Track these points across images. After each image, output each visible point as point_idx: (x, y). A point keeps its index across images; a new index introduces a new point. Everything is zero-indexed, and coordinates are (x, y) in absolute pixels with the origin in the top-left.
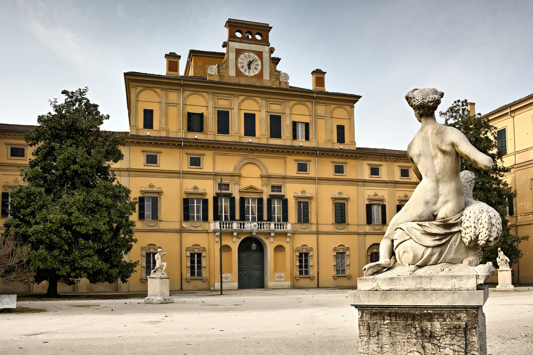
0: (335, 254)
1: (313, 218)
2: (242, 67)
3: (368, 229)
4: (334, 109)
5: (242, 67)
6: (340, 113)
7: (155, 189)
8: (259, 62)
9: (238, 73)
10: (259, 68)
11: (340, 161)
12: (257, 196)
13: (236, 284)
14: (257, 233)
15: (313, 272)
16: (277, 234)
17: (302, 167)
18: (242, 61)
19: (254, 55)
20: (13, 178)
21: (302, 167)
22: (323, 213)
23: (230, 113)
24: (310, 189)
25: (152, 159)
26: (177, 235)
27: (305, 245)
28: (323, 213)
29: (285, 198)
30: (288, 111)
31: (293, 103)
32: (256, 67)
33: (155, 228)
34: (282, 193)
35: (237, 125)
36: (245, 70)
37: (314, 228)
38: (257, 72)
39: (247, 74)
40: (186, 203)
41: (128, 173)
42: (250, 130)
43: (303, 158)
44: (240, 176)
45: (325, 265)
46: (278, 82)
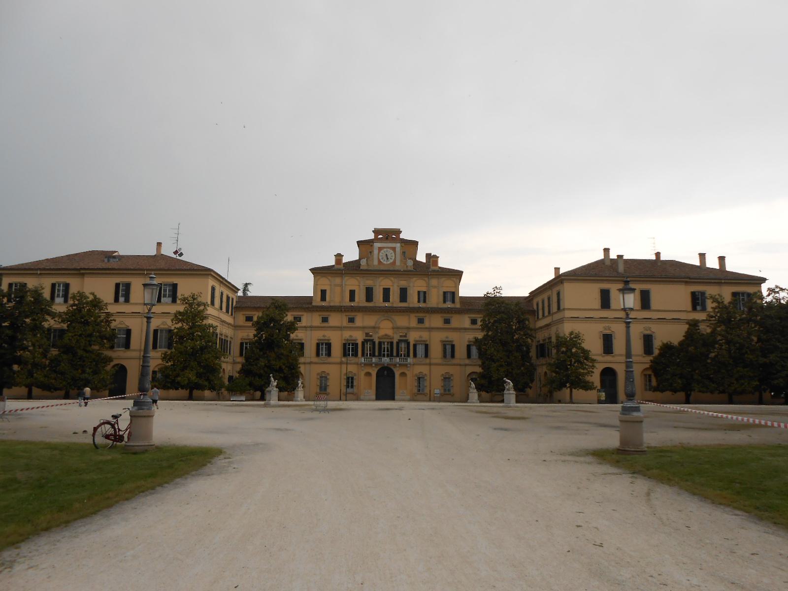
0: (442, 378)
3: (467, 361)
5: (382, 258)
6: (447, 284)
7: (326, 338)
8: (393, 254)
9: (380, 262)
10: (393, 258)
11: (447, 316)
12: (390, 340)
13: (374, 397)
14: (388, 364)
15: (427, 391)
16: (400, 365)
17: (421, 321)
20: (246, 334)
21: (421, 321)
22: (436, 351)
25: (325, 320)
26: (339, 366)
27: (421, 372)
29: (409, 341)
30: (411, 285)
31: (415, 279)
33: (326, 361)
34: (407, 338)
35: (378, 295)
38: (392, 261)
41: (310, 329)
42: (386, 298)
43: (421, 315)
44: (379, 328)
46: (406, 266)
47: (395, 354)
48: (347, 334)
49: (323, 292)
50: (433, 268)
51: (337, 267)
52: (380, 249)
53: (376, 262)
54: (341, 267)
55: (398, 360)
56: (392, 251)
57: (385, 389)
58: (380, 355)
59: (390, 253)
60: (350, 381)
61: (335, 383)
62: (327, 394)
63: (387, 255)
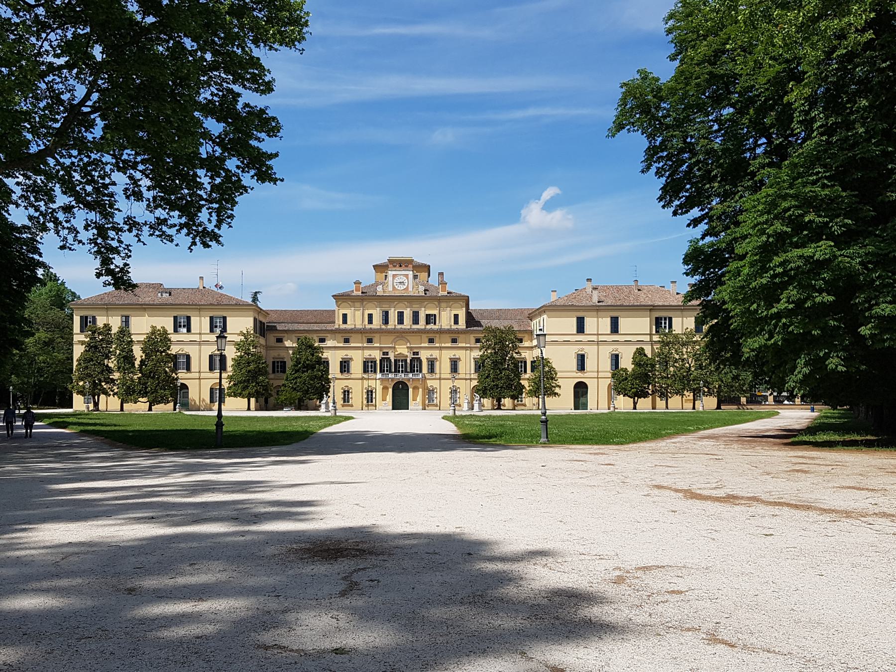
1: (437, 369)
16: (413, 380)
22: (444, 367)
24: (435, 354)
28: (444, 367)
37: (438, 376)
40: (366, 365)
42: (401, 321)
45: (444, 397)
47: (409, 370)
48: (367, 353)
49: (345, 316)
50: (441, 293)
51: (355, 293)
52: (394, 276)
53: (390, 289)
54: (360, 293)
55: (410, 375)
57: (400, 402)
58: (397, 371)
59: (404, 279)
60: (370, 394)
61: (357, 397)
62: (352, 406)
63: (401, 282)
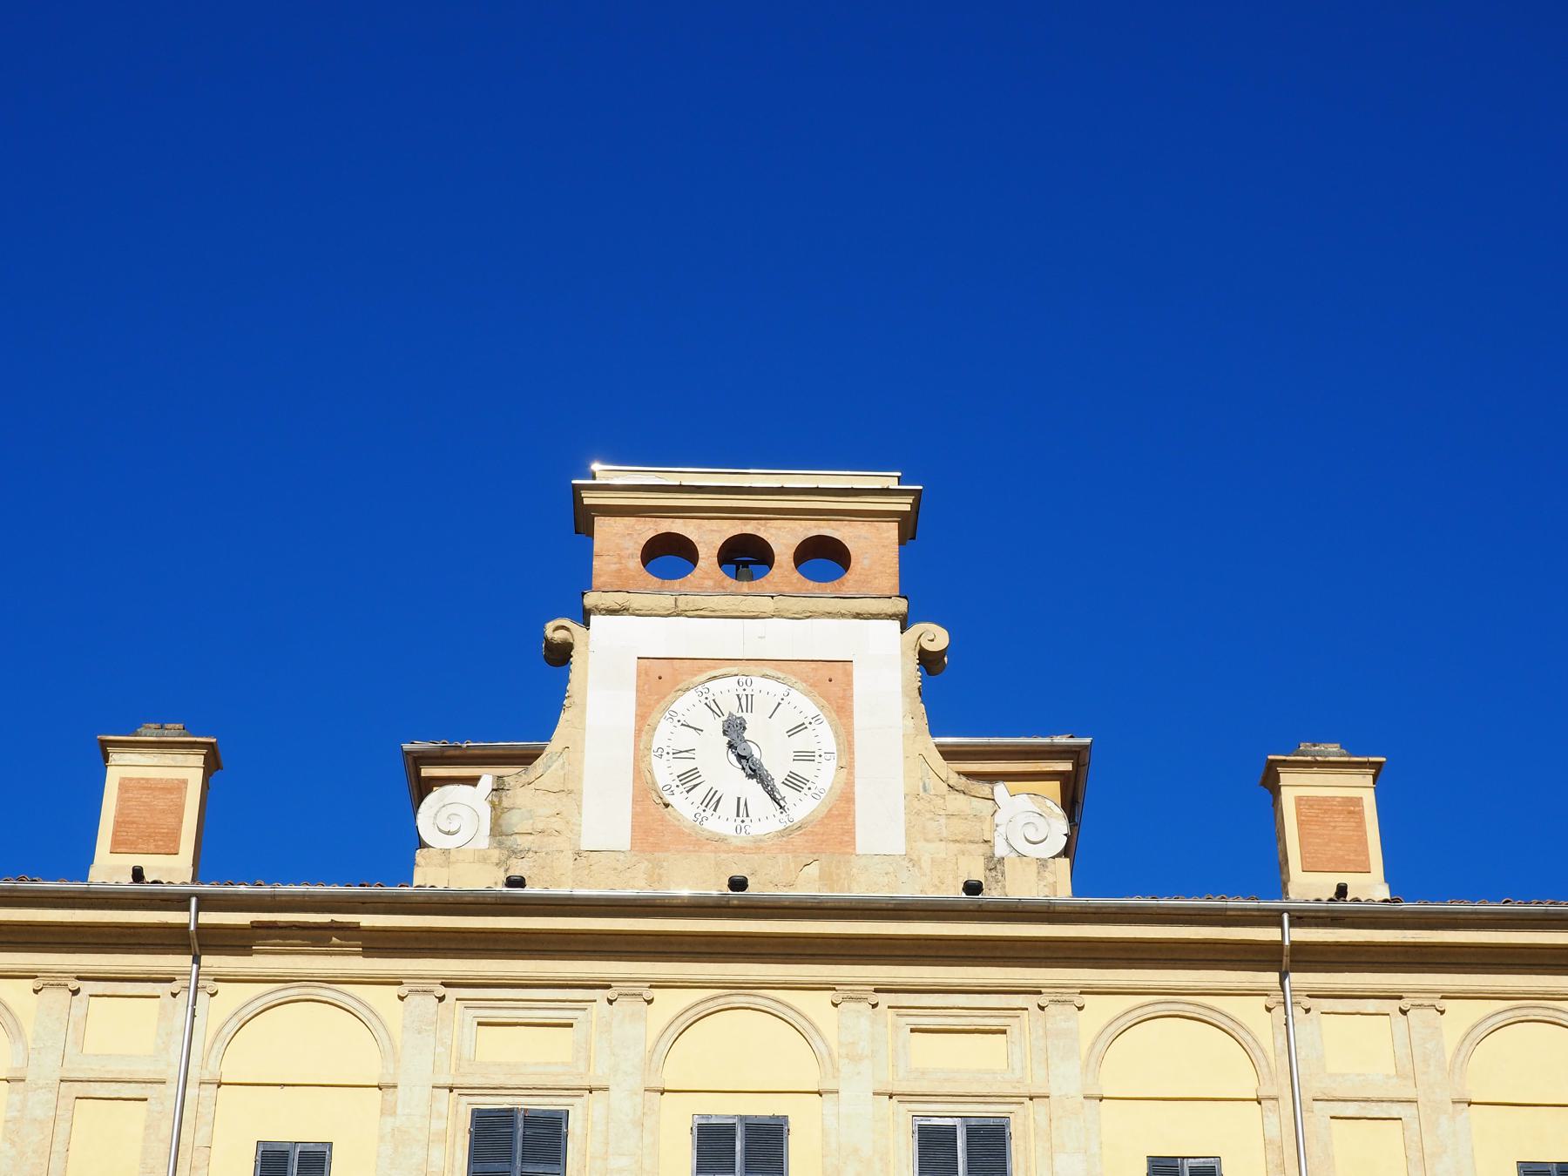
2: (689, 779)
4: (1479, 1035)
5: (689, 779)
8: (823, 737)
10: (824, 775)
18: (686, 739)
19: (779, 689)
23: (575, 1127)
30: (1066, 1080)
32: (802, 769)
36: (713, 801)
38: (801, 807)
39: (721, 823)
52: (659, 680)
56: (802, 705)
